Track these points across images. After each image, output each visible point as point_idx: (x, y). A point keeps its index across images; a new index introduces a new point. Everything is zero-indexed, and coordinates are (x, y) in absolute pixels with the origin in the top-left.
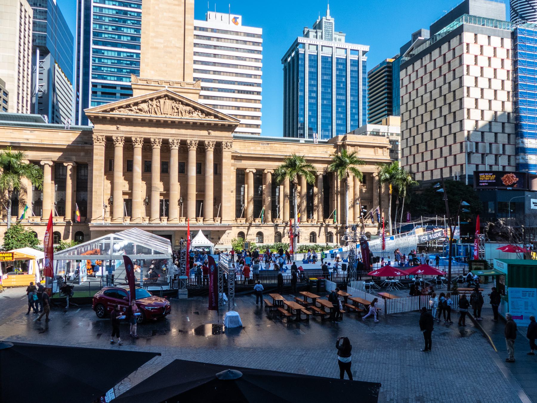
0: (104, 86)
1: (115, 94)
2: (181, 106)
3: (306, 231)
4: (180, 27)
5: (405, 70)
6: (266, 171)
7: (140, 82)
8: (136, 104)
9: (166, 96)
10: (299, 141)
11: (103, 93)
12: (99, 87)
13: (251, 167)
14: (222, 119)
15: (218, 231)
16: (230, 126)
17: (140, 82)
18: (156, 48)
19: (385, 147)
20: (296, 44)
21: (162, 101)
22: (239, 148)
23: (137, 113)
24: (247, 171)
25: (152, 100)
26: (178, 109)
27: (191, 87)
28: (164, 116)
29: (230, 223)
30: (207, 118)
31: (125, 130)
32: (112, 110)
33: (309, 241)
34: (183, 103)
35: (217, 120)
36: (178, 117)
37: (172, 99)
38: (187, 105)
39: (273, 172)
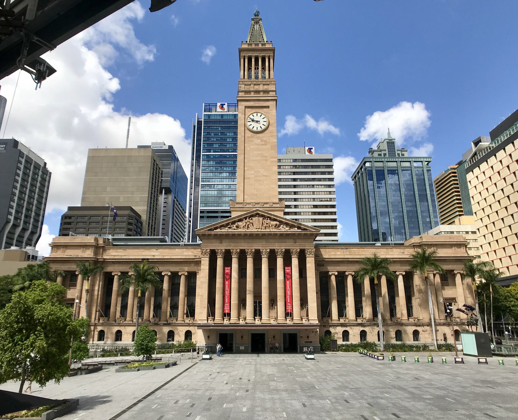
0: (209, 212)
6: (347, 273)
7: (237, 206)
10: (374, 244)
11: (208, 217)
15: (307, 330)
17: (237, 206)
18: (249, 178)
24: (330, 273)
27: (278, 206)
28: (256, 230)
30: (292, 230)
34: (271, 219)
36: (267, 230)
37: (262, 216)
38: (275, 220)
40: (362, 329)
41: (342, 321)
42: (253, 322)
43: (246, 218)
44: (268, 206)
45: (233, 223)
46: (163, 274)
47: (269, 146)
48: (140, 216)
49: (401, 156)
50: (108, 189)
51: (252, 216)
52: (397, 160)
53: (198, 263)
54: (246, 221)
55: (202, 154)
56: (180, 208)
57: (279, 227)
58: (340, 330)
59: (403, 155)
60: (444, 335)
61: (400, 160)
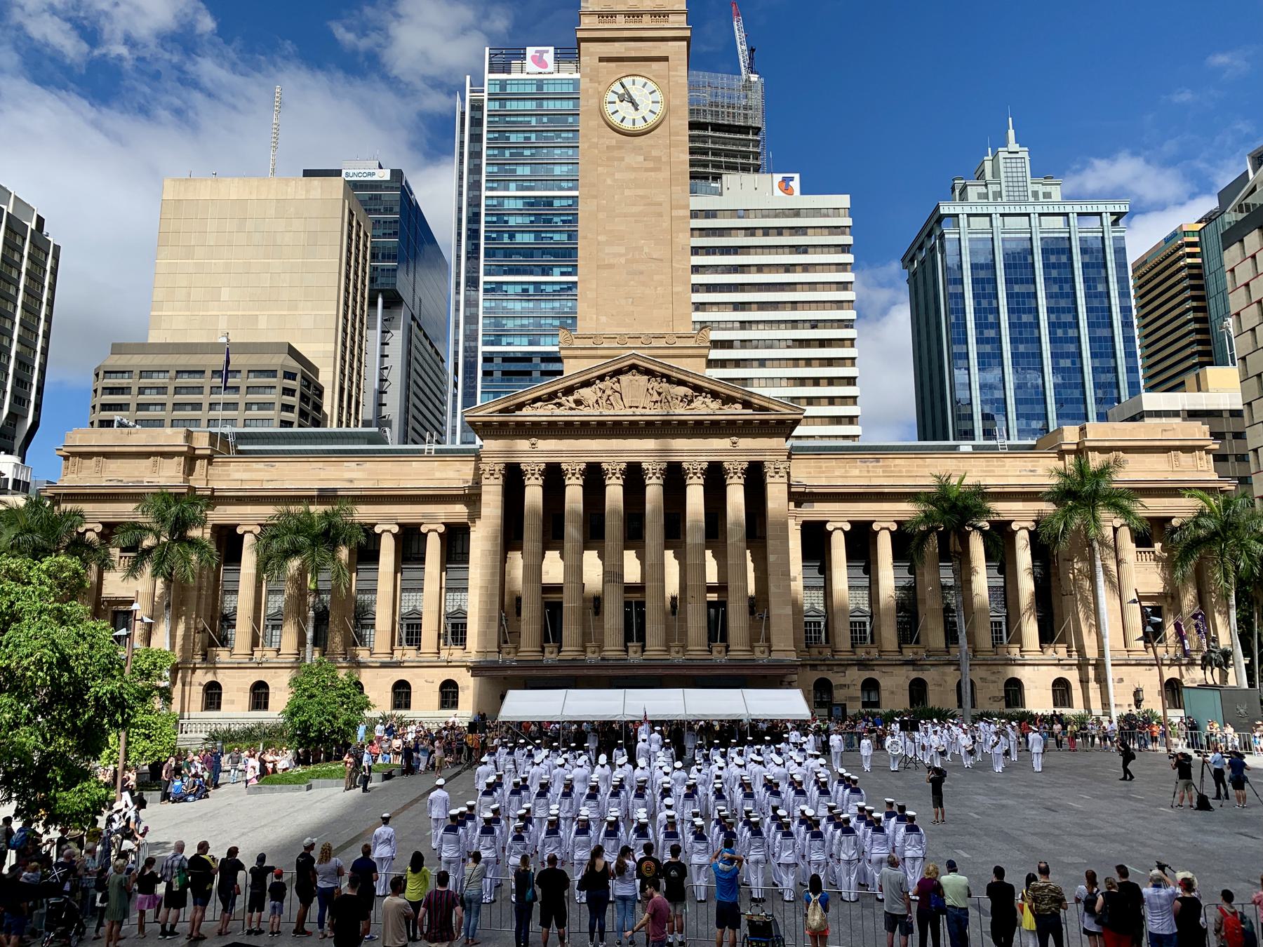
0: (507, 358)
1: (529, 373)
2: (665, 385)
3: (993, 678)
4: (660, 215)
5: (1237, 245)
7: (578, 343)
8: (569, 391)
9: (633, 367)
10: (955, 448)
11: (504, 373)
12: (498, 361)
13: (838, 518)
14: (763, 409)
16: (781, 423)
17: (578, 343)
18: (611, 266)
19: (1201, 448)
20: (935, 218)
21: (622, 378)
22: (808, 474)
23: (571, 409)
25: (602, 378)
26: (659, 394)
27: (691, 343)
28: (630, 412)
29: (793, 657)
31: (550, 448)
32: (520, 406)
33: (1003, 703)
34: (670, 380)
35: (750, 411)
37: (648, 372)
39: (894, 527)
40: (914, 675)
41: (861, 653)
42: (622, 655)
43: (602, 378)
44: (662, 343)
45: (569, 391)
46: (378, 530)
47: (664, 175)
48: (315, 371)
49: (1041, 199)
50: (225, 294)
51: (618, 372)
52: (1030, 210)
53: (472, 498)
54: (602, 385)
55: (484, 193)
56: (429, 348)
57: (691, 401)
58: (856, 677)
59: (1047, 195)
60: (1137, 693)
61: (1039, 209)
